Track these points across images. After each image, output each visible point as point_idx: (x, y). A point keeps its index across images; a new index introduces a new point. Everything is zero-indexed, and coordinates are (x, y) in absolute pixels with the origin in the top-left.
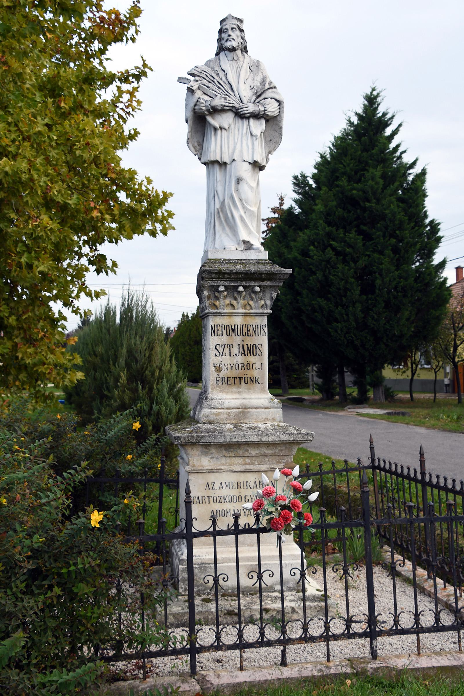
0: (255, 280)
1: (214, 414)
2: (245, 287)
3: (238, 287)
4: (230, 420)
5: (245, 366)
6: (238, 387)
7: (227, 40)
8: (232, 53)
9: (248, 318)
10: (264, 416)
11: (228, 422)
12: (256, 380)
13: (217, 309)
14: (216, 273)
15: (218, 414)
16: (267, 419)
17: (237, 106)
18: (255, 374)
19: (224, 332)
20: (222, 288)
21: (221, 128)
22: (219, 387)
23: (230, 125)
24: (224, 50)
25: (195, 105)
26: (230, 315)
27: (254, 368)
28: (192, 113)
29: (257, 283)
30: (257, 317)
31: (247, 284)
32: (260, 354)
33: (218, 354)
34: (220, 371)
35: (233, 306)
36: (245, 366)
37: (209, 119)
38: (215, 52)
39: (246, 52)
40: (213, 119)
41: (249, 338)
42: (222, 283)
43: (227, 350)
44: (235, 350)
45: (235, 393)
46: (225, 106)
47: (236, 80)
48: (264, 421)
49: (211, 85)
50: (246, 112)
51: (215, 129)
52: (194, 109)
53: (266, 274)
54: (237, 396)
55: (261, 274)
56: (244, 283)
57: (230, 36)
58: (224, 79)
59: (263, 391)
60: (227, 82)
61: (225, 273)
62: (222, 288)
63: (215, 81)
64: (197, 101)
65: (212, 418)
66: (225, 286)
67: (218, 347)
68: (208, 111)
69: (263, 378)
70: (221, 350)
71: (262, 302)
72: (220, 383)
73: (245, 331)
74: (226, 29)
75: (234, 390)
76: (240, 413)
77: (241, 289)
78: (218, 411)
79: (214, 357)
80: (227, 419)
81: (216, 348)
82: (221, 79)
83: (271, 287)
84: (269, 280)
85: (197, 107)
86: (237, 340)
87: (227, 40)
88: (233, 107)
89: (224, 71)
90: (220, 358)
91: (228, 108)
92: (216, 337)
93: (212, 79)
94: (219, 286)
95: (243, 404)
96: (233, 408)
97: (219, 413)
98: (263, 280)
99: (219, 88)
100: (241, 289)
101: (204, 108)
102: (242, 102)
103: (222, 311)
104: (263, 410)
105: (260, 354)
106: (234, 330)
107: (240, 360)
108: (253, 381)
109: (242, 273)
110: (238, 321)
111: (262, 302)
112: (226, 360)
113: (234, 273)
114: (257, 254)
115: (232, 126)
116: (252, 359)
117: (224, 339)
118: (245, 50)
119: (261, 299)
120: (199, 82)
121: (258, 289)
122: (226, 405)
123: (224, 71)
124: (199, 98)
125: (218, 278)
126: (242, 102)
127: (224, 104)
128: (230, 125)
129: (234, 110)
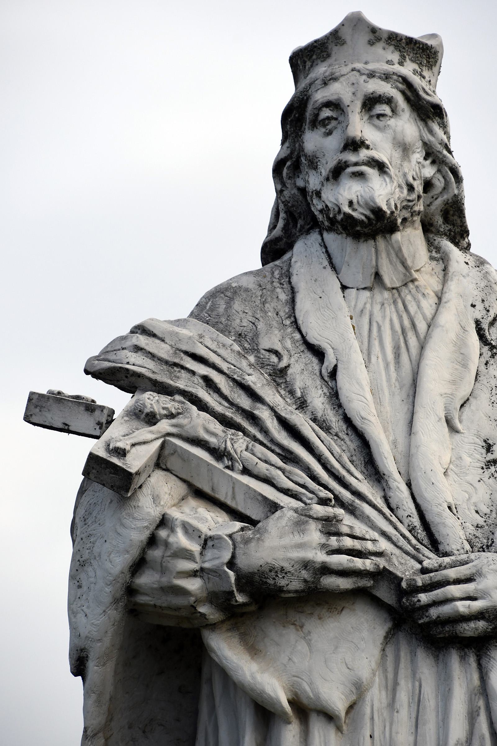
8: (366, 249)
17: (405, 568)
21: (305, 710)
23: (359, 690)
24: (313, 224)
25: (139, 565)
28: (115, 614)
37: (227, 650)
38: (261, 234)
39: (459, 234)
40: (253, 650)
46: (325, 570)
47: (394, 405)
50: (462, 607)
51: (266, 715)
52: (131, 591)
57: (354, 145)
58: (318, 400)
68: (221, 600)
74: (335, 105)
82: (302, 405)
85: (146, 579)
87: (337, 172)
88: (382, 575)
89: (318, 353)
91: (344, 583)
93: (245, 402)
99: (289, 457)
115: (376, 697)
118: (448, 222)
120: (164, 426)
126: (435, 544)
128: (359, 690)
129: (385, 593)
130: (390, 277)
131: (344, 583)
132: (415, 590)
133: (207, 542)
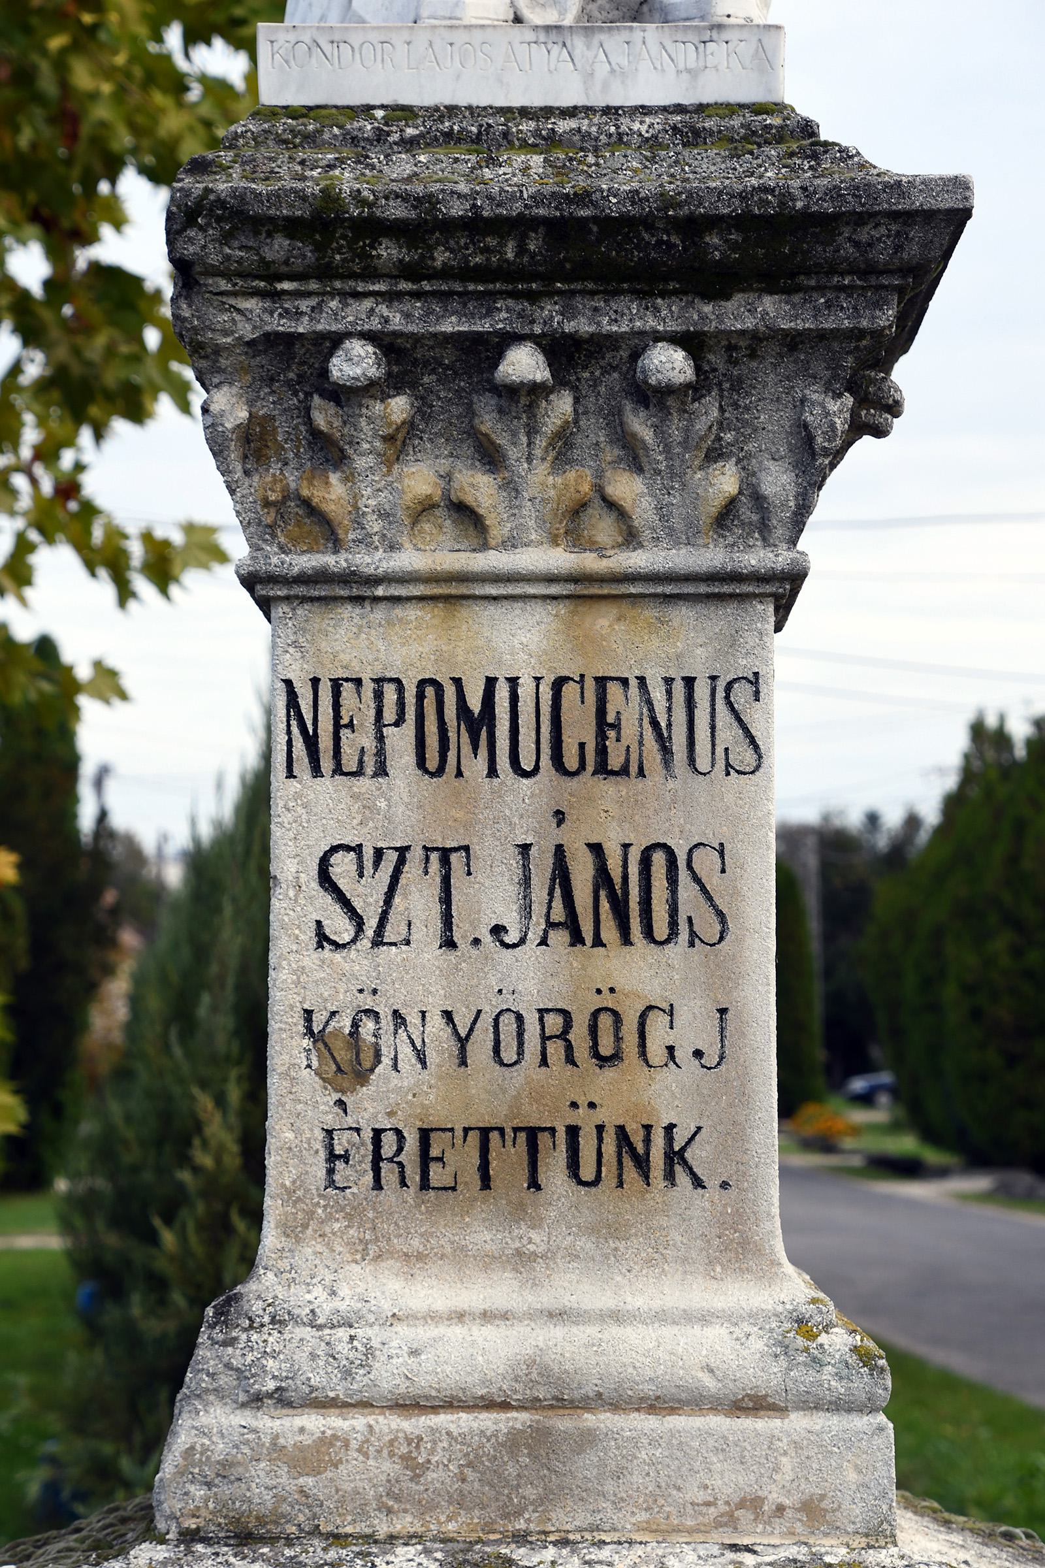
0: (647, 283)
1: (276, 1449)
2: (563, 353)
3: (496, 346)
4: (425, 1508)
5: (579, 1034)
6: (519, 1213)
9: (603, 621)
10: (728, 1481)
11: (404, 1523)
12: (675, 1157)
13: (336, 544)
14: (292, 227)
15: (317, 1457)
16: (753, 1503)
18: (666, 1097)
19: (401, 740)
20: (355, 363)
22: (353, 1215)
26: (451, 593)
27: (656, 1052)
29: (669, 315)
30: (682, 615)
31: (582, 326)
32: (708, 927)
33: (340, 927)
34: (362, 1076)
35: (466, 515)
36: (579, 1034)
41: (609, 790)
42: (357, 313)
43: (418, 899)
44: (491, 896)
45: (489, 1261)
48: (729, 1521)
53: (742, 222)
54: (501, 1290)
55: (694, 226)
56: (549, 314)
59: (735, 1249)
61: (374, 227)
62: (355, 363)
65: (263, 1487)
66: (388, 345)
67: (342, 867)
69: (736, 1135)
70: (367, 895)
71: (725, 481)
72: (356, 1176)
73: (579, 728)
75: (483, 1236)
76: (513, 1442)
77: (523, 364)
78: (314, 1423)
79: (311, 958)
80: (392, 1499)
81: (325, 879)
83: (793, 342)
84: (776, 279)
86: (510, 810)
90: (359, 962)
92: (327, 788)
94: (335, 341)
95: (536, 1368)
96: (451, 1404)
97: (326, 1442)
98: (716, 283)
100: (523, 364)
103: (369, 561)
104: (718, 1422)
105: (708, 927)
106: (478, 724)
107: (534, 976)
108: (642, 1164)
109: (520, 225)
110: (518, 645)
111: (725, 481)
112: (416, 977)
113: (450, 226)
114: (687, 55)
116: (638, 972)
117: (400, 804)
119: (714, 455)
121: (669, 363)
122: (388, 1375)
125: (325, 272)
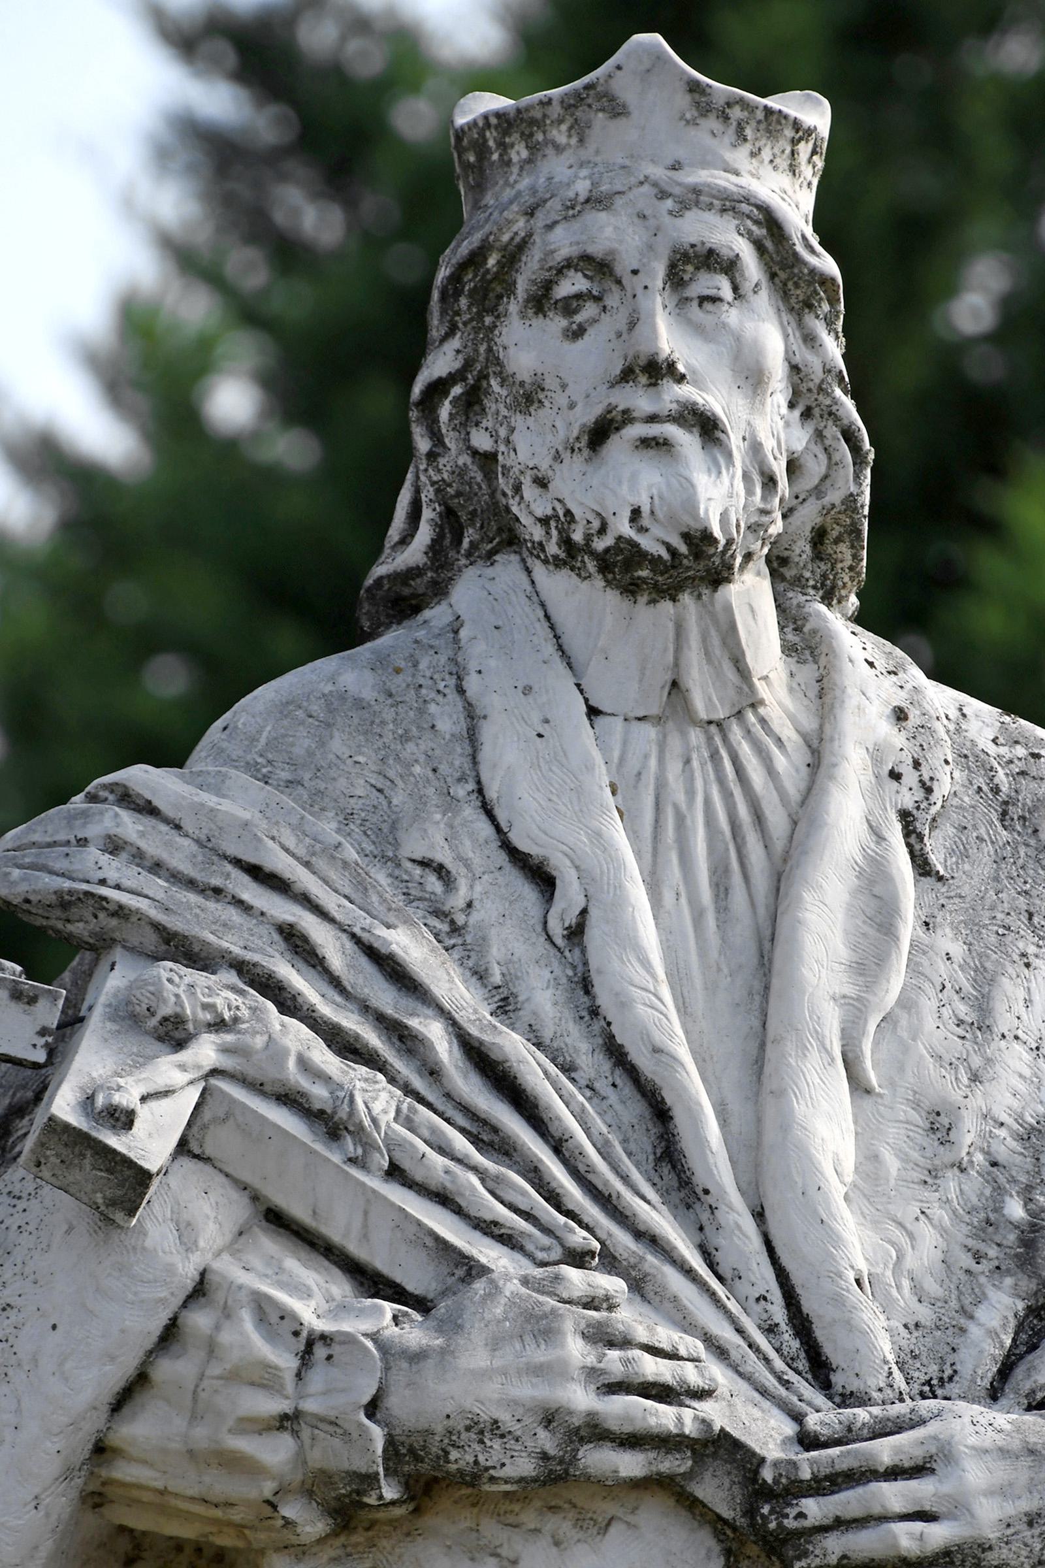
7: (600, 434)
17: (767, 1434)
46: (595, 1432)
49: (376, 1100)
52: (101, 1450)
58: (544, 997)
60: (591, 1062)
63: (435, 1033)
64: (170, 1334)
74: (600, 267)
85: (142, 1429)
87: (600, 434)
89: (543, 879)
91: (631, 1464)
101: (276, 1452)
102: (820, 1369)
120: (206, 1051)
123: (543, 879)
124: (200, 1290)
127: (582, 1399)
130: (705, 698)
131: (631, 1464)
132: (793, 1489)
133: (311, 1346)
